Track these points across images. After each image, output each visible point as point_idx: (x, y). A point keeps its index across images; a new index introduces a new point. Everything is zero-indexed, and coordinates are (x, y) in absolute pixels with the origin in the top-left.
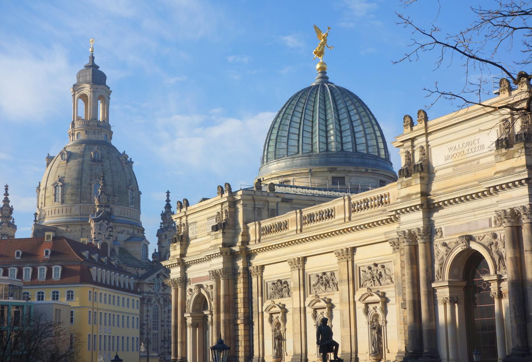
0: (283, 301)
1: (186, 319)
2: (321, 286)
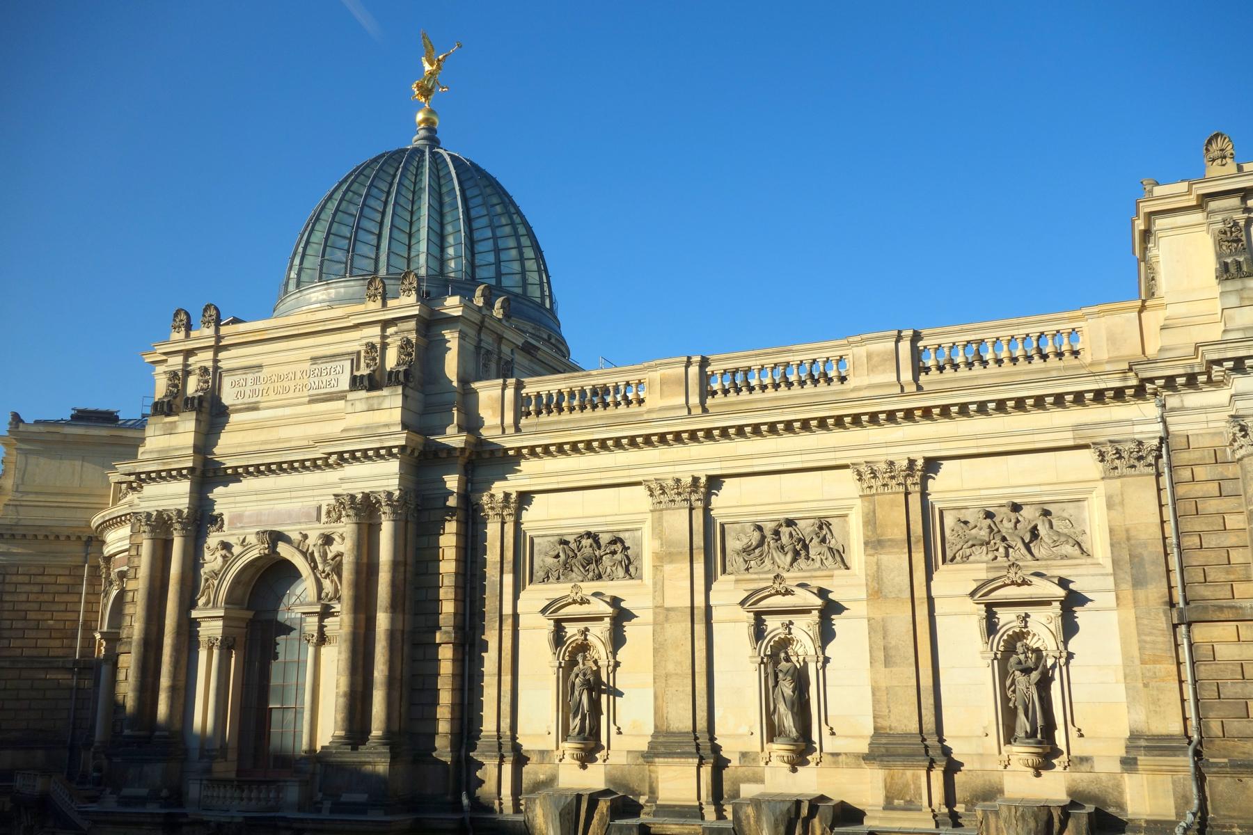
0: (610, 588)
1: (195, 623)
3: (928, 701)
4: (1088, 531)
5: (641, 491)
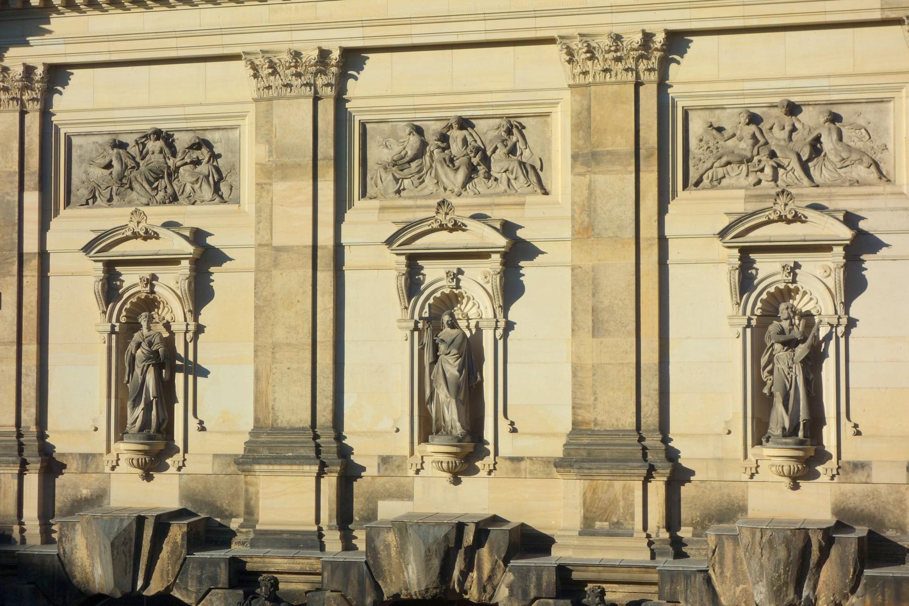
0: (190, 216)
2: (444, 173)
3: (650, 385)
4: (890, 146)
5: (240, 68)
